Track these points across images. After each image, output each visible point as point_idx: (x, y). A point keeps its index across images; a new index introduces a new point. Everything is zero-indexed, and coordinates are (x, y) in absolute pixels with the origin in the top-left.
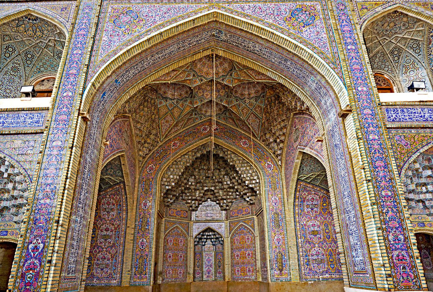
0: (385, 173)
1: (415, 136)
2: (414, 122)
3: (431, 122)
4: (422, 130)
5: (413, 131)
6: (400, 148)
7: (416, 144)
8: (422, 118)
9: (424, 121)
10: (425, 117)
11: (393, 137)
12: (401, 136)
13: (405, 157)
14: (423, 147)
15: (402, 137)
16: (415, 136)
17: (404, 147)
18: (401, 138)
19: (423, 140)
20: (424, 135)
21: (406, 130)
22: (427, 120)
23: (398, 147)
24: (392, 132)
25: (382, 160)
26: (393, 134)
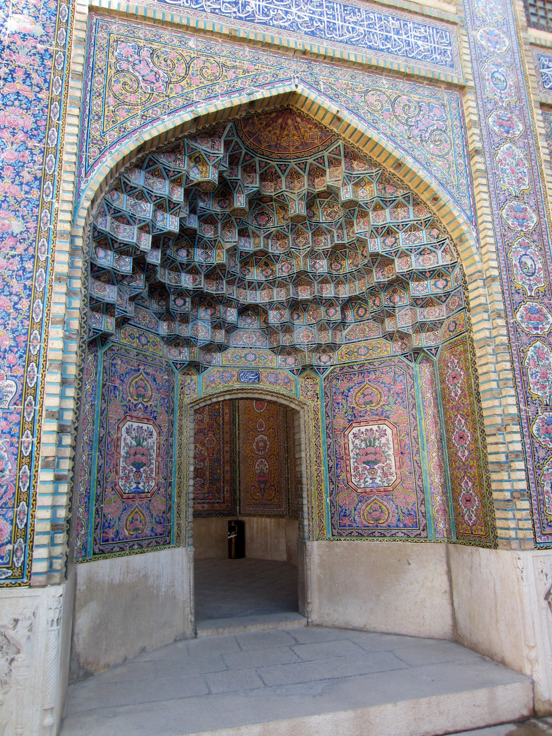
0: (27, 152)
1: (192, 59)
2: (204, 14)
3: (262, 26)
4: (227, 48)
5: (192, 43)
6: (125, 84)
7: (189, 85)
8: (235, 10)
9: (241, 18)
10: (248, 8)
11: (109, 46)
12: (140, 48)
13: (133, 117)
14: (210, 98)
15: (145, 53)
16: (192, 59)
17: (142, 84)
18: (138, 54)
19: (216, 78)
20: (229, 63)
21: (167, 34)
22: (250, 18)
23: (117, 81)
24: (114, 27)
25: (28, 109)
26: (114, 37)
